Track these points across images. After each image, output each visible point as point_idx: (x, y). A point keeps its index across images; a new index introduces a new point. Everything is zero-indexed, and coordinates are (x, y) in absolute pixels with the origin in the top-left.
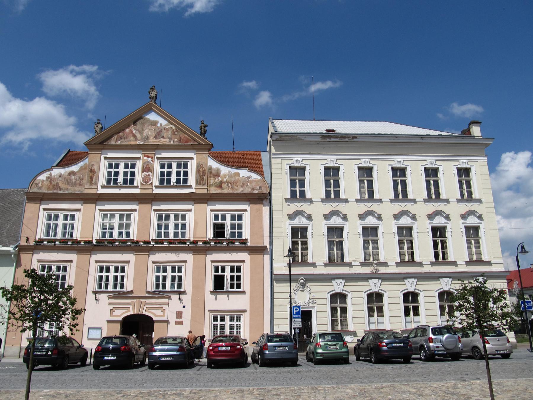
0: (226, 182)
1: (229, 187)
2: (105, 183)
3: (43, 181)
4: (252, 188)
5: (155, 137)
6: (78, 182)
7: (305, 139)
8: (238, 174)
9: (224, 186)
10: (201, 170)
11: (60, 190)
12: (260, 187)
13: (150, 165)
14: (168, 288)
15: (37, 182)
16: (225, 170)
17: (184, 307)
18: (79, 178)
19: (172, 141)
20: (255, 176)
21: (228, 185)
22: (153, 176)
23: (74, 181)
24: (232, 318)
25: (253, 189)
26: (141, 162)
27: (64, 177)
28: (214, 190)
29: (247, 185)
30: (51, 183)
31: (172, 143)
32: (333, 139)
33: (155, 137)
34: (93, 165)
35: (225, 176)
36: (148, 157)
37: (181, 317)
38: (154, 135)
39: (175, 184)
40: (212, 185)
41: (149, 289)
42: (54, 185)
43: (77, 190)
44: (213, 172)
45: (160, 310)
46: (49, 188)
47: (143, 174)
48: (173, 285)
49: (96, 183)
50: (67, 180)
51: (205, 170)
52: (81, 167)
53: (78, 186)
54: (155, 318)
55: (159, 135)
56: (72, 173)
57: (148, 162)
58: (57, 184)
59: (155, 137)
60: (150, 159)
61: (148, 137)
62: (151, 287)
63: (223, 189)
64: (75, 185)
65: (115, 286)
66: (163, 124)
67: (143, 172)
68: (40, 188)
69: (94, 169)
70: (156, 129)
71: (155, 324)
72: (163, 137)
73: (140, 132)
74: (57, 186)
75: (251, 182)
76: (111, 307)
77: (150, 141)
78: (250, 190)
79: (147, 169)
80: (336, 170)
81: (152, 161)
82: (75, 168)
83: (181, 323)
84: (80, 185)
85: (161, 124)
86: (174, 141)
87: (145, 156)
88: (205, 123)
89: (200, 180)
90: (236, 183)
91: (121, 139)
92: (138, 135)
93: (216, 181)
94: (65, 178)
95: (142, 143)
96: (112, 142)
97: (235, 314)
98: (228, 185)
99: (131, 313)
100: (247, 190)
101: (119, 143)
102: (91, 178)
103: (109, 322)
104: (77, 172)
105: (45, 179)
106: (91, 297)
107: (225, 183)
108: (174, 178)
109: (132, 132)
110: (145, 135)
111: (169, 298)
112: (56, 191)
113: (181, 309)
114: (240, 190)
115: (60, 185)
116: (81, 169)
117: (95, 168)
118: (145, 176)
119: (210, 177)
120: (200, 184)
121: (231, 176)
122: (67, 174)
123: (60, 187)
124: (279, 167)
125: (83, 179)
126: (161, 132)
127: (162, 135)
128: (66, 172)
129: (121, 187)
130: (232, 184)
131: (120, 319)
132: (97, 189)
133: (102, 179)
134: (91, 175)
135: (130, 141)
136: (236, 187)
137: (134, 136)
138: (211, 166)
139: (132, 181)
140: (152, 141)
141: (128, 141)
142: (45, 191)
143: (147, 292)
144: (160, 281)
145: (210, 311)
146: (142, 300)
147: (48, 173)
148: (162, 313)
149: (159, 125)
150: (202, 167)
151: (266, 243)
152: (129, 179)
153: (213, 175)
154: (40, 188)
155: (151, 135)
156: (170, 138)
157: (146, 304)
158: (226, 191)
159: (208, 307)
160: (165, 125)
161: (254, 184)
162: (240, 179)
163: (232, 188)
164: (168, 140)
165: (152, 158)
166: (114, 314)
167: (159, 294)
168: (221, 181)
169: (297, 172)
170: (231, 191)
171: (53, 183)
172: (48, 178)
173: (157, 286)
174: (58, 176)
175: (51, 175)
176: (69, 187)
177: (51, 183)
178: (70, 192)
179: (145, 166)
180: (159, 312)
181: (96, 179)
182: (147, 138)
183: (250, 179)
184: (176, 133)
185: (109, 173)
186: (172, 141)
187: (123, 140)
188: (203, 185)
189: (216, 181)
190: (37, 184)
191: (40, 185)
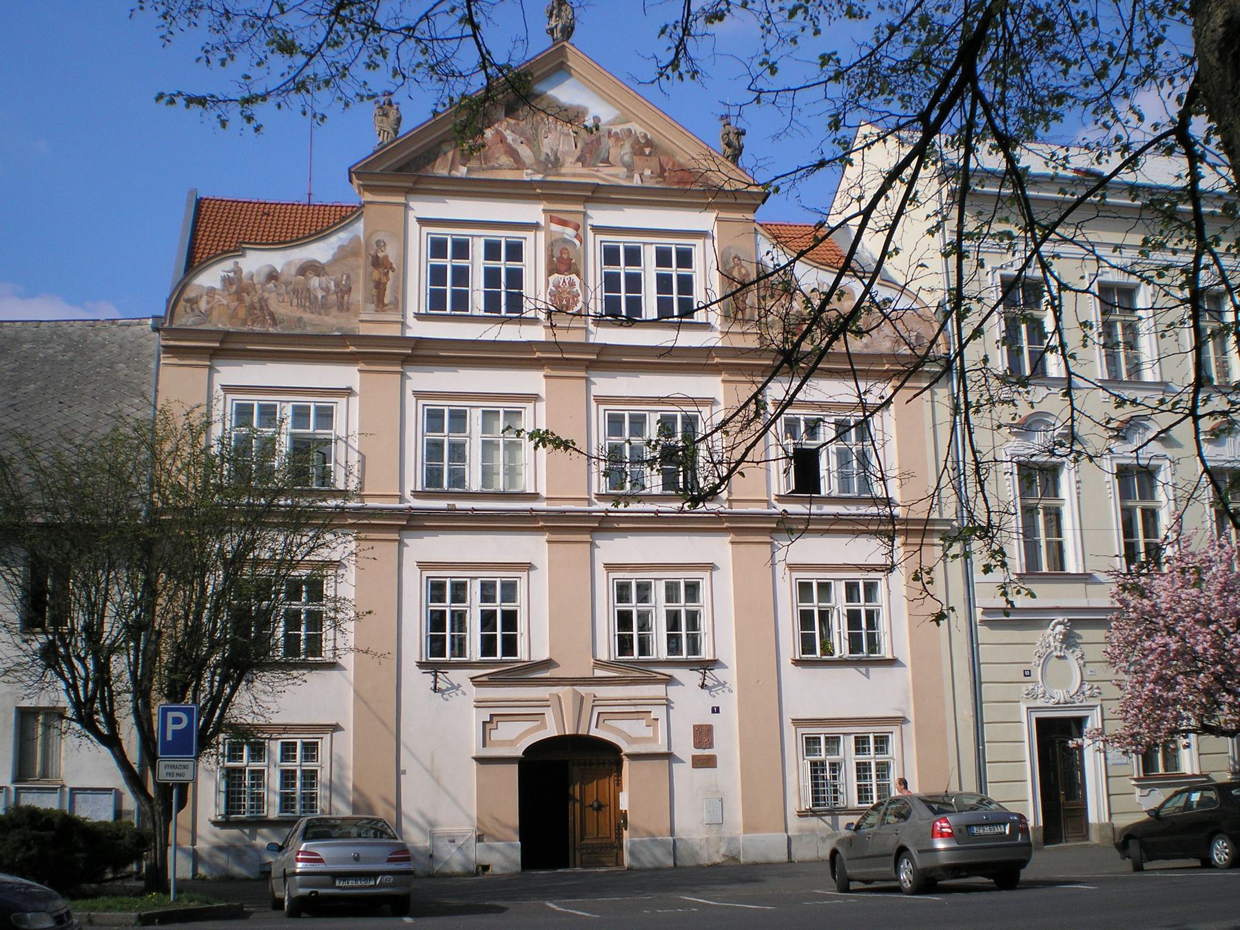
3: (211, 291)
17: (716, 710)
18: (337, 285)
19: (637, 177)
22: (585, 285)
23: (320, 294)
26: (541, 235)
27: (283, 278)
30: (240, 300)
31: (636, 181)
34: (380, 244)
36: (564, 223)
38: (578, 153)
41: (603, 655)
43: (332, 322)
45: (644, 723)
47: (552, 279)
50: (295, 291)
52: (341, 248)
53: (334, 312)
54: (626, 748)
56: (310, 268)
57: (565, 241)
58: (263, 303)
59: (578, 160)
60: (569, 232)
61: (557, 159)
64: (322, 307)
65: (488, 646)
67: (550, 272)
69: (386, 257)
72: (606, 161)
74: (261, 310)
77: (563, 170)
81: (577, 236)
82: (321, 251)
83: (706, 762)
84: (343, 307)
85: (597, 119)
86: (644, 176)
87: (552, 220)
92: (525, 152)
94: (287, 284)
95: (538, 177)
96: (441, 170)
97: (871, 731)
99: (551, 730)
101: (462, 171)
102: (380, 286)
103: (481, 760)
105: (218, 285)
106: (416, 682)
109: (503, 140)
111: (669, 681)
115: (274, 305)
116: (343, 254)
117: (391, 252)
118: (557, 287)
122: (293, 270)
123: (272, 315)
127: (603, 155)
128: (289, 264)
131: (518, 751)
132: (403, 324)
135: (500, 168)
137: (513, 153)
139: (516, 302)
140: (572, 171)
143: (599, 664)
145: (797, 722)
146: (582, 690)
147: (228, 265)
148: (649, 732)
152: (506, 297)
154: (207, 315)
155: (567, 153)
156: (630, 168)
160: (613, 123)
164: (622, 171)
165: (577, 228)
166: (495, 735)
171: (247, 299)
172: (227, 281)
173: (625, 645)
174: (262, 278)
175: (238, 271)
176: (307, 316)
177: (240, 300)
179: (557, 254)
180: (636, 728)
182: (555, 162)
186: (637, 177)
187: (474, 163)
190: (193, 302)
191: (203, 305)
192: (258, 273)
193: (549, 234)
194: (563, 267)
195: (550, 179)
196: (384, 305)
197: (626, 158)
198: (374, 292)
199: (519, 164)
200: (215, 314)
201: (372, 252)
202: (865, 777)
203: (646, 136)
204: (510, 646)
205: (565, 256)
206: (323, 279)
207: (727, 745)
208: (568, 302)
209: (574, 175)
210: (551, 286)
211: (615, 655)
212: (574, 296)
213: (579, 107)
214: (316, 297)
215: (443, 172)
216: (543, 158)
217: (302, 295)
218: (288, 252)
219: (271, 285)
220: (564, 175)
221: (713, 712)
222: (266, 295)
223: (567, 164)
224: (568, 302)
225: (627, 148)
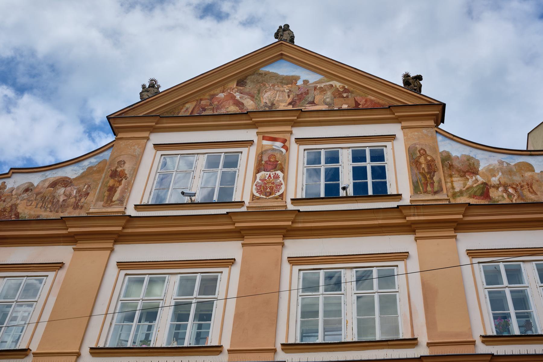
0: (500, 184)
8: (530, 168)
10: (422, 160)
13: (278, 156)
18: (79, 191)
22: (285, 178)
26: (253, 150)
35: (492, 172)
47: (259, 175)
51: (433, 160)
55: (300, 99)
66: (311, 81)
67: (258, 171)
87: (264, 138)
90: (530, 185)
98: (506, 191)
102: (112, 190)
104: (74, 179)
107: (497, 187)
118: (263, 180)
119: (451, 176)
120: (426, 192)
121: (509, 172)
122: (47, 184)
125: (88, 194)
127: (310, 99)
128: (44, 181)
134: (111, 182)
138: (448, 153)
149: (300, 83)
153: (459, 171)
162: (536, 177)
168: (485, 184)
174: (21, 190)
179: (265, 158)
181: (123, 192)
184: (345, 95)
188: (436, 193)
189: (470, 183)
192: (18, 188)
193: (260, 145)
196: (112, 201)
197: (328, 100)
198: (106, 194)
201: (113, 168)
203: (344, 87)
205: (272, 160)
206: (68, 189)
208: (271, 188)
210: (258, 180)
212: (277, 186)
213: (293, 76)
214: (58, 201)
219: (25, 195)
225: (329, 93)
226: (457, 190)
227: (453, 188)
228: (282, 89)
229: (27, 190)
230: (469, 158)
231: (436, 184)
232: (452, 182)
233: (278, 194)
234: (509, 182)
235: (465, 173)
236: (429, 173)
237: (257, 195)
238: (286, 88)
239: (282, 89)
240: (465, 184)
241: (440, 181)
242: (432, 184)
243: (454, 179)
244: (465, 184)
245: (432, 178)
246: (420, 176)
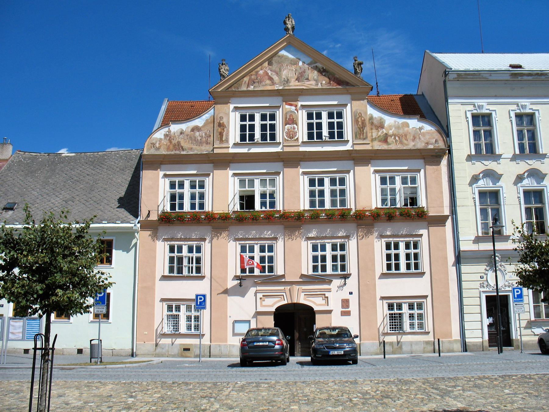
0: (393, 135)
1: (396, 141)
2: (238, 140)
3: (161, 139)
4: (426, 141)
5: (298, 79)
6: (204, 139)
7: (491, 78)
8: (407, 125)
9: (390, 140)
10: (359, 120)
11: (183, 150)
12: (436, 141)
14: (329, 271)
15: (154, 142)
16: (389, 121)
17: (351, 293)
18: (206, 134)
19: (320, 84)
20: (428, 128)
21: (395, 138)
22: (298, 129)
23: (199, 138)
24: (411, 307)
25: (427, 143)
27: (186, 134)
28: (378, 146)
29: (420, 138)
30: (171, 142)
31: (319, 86)
32: (525, 78)
33: (298, 79)
34: (221, 118)
35: (390, 127)
36: (291, 105)
37: (348, 307)
38: (296, 77)
39: (327, 139)
40: (375, 138)
41: (305, 273)
42: (174, 145)
43: (205, 149)
44: (375, 122)
46: (168, 149)
47: (286, 127)
48: (335, 268)
49: (227, 141)
51: (364, 120)
52: (207, 120)
53: (205, 144)
54: (316, 308)
55: (301, 76)
56: (196, 129)
57: (292, 112)
58: (179, 143)
59: (296, 80)
60: (293, 108)
61: (288, 80)
62: (307, 268)
63: (390, 144)
64: (200, 143)
68: (158, 149)
69: (223, 123)
70: (298, 68)
71: (317, 316)
73: (277, 74)
74: (178, 146)
75: (424, 134)
76: (260, 295)
77: (291, 84)
78: (423, 144)
79: (291, 120)
80: (531, 117)
82: (199, 122)
83: (348, 314)
88: (359, 60)
89: (360, 132)
90: (406, 135)
91: (254, 83)
92: (276, 78)
93: (380, 133)
94: (187, 136)
95: (281, 88)
98: (395, 138)
99: (285, 302)
100: (420, 145)
101: (251, 88)
102: (221, 134)
105: (163, 137)
108: (325, 132)
109: (267, 74)
110: (284, 77)
112: (177, 152)
113: (347, 296)
114: (410, 145)
115: (182, 144)
117: (224, 121)
118: (288, 130)
119: (372, 129)
121: (398, 128)
122: (190, 130)
123: (182, 147)
124: (459, 113)
126: (304, 72)
127: (306, 77)
128: (188, 128)
129: (257, 145)
130: (401, 137)
131: (273, 309)
133: (234, 135)
134: (220, 130)
135: (266, 85)
136: (405, 142)
137: (271, 79)
138: (372, 115)
139: (273, 137)
140: (294, 85)
141: (263, 86)
142: (164, 153)
144: (319, 262)
145: (383, 298)
150: (361, 116)
151: (447, 212)
153: (376, 126)
154: (158, 149)
156: (316, 80)
157: (304, 291)
158: (393, 147)
159: (380, 293)
161: (427, 137)
162: (410, 131)
163: (401, 142)
164: (313, 83)
166: (264, 303)
167: (318, 278)
168: (386, 134)
169: (482, 122)
170: (399, 147)
171: (173, 142)
172: (166, 136)
173: (315, 268)
174: (179, 133)
175: (169, 131)
177: (171, 142)
178: (195, 152)
179: (288, 117)
182: (287, 81)
183: (422, 131)
185: (243, 128)
186: (320, 84)
187: (256, 84)
188: (364, 139)
189: (380, 133)
191: (157, 145)
194: (291, 122)
195: (286, 88)
197: (315, 77)
199: (273, 83)
200: (162, 147)
202: (413, 319)
204: (271, 269)
207: (353, 307)
208: (293, 135)
209: (295, 86)
211: (311, 272)
215: (244, 88)
216: (283, 79)
217: (193, 139)
218: (188, 123)
220: (291, 86)
221: (350, 294)
222: (180, 140)
223: (292, 82)
224: (293, 135)
226: (374, 137)
227: (372, 136)
228: (291, 68)
229: (181, 133)
230: (381, 119)
231: (365, 134)
232: (372, 133)
233: (296, 138)
234: (397, 134)
235: (378, 127)
236: (362, 128)
237: (286, 138)
238: (293, 68)
239: (291, 68)
240: (377, 134)
241: (366, 133)
242: (363, 134)
243: (373, 131)
244: (377, 134)
245: (363, 131)
246: (358, 129)
